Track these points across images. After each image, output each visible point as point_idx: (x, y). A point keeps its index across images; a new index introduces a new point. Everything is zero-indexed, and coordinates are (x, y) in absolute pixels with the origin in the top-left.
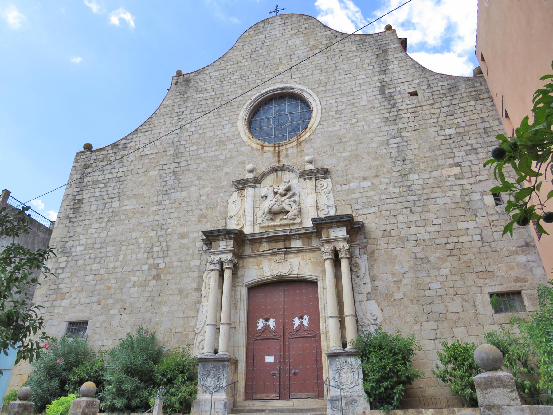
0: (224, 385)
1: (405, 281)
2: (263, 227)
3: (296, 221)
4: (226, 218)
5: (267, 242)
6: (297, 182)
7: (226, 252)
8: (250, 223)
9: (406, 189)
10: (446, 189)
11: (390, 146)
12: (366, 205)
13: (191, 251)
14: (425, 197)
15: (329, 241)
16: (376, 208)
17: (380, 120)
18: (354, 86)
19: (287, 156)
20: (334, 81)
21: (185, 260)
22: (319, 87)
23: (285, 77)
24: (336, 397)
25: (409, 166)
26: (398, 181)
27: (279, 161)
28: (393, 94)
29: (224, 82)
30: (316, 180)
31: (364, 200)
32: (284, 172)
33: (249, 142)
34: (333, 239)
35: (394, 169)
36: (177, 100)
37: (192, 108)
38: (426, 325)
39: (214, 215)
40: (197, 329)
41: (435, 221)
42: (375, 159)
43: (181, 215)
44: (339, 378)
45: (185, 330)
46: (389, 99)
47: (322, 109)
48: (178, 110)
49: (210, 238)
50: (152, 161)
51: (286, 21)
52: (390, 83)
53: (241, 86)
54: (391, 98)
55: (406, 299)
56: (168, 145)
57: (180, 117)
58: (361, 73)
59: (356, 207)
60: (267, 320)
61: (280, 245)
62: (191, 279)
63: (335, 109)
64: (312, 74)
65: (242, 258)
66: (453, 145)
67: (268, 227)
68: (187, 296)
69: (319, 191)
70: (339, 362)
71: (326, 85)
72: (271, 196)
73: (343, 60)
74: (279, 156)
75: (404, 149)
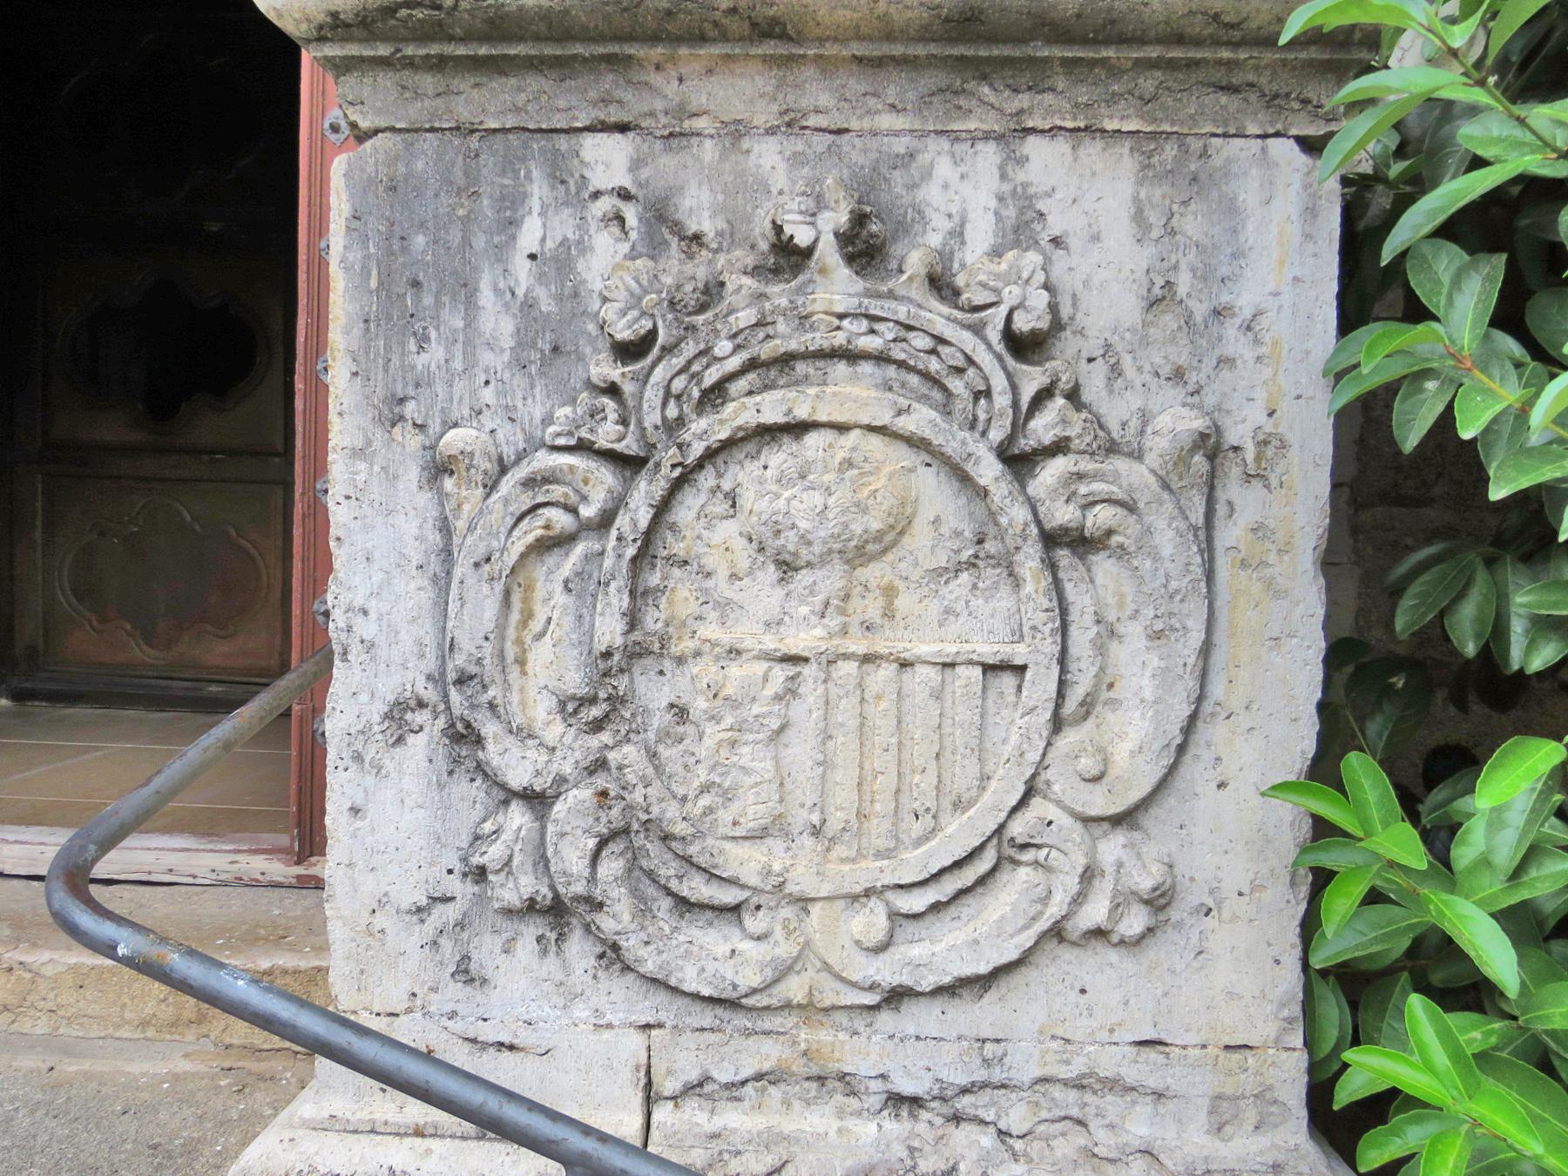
44: (600, 704)
70: (662, 224)
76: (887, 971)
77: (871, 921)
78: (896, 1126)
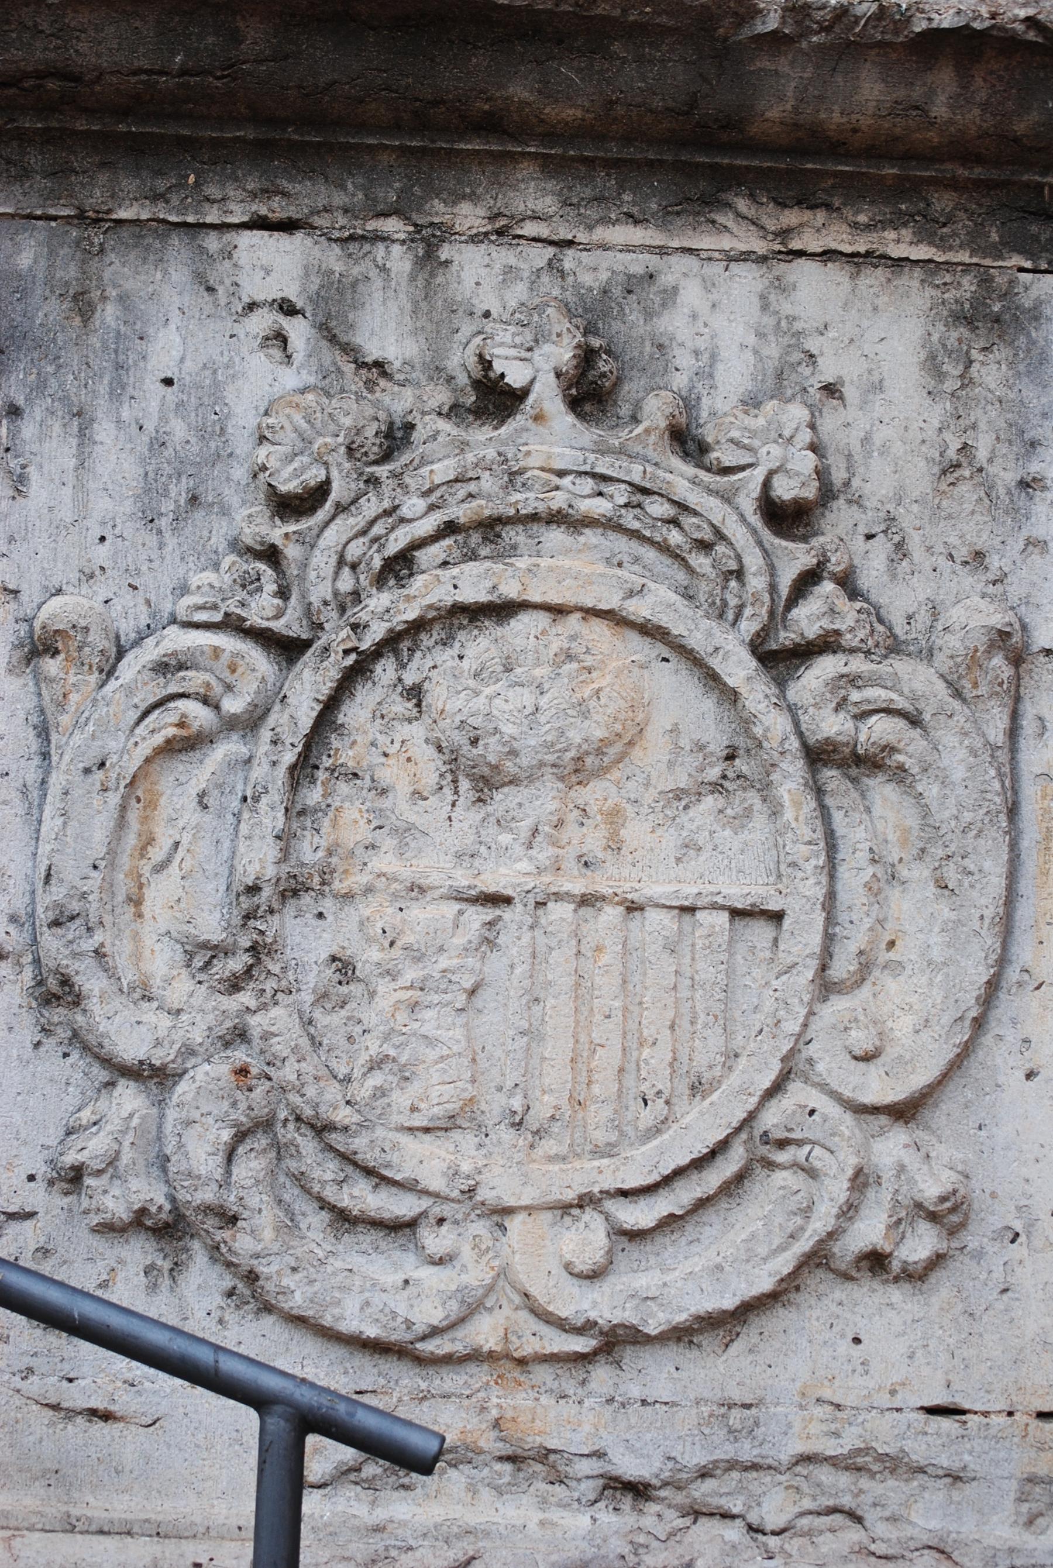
44: (242, 958)
76: (603, 1304)
77: (586, 1239)
78: (615, 1522)
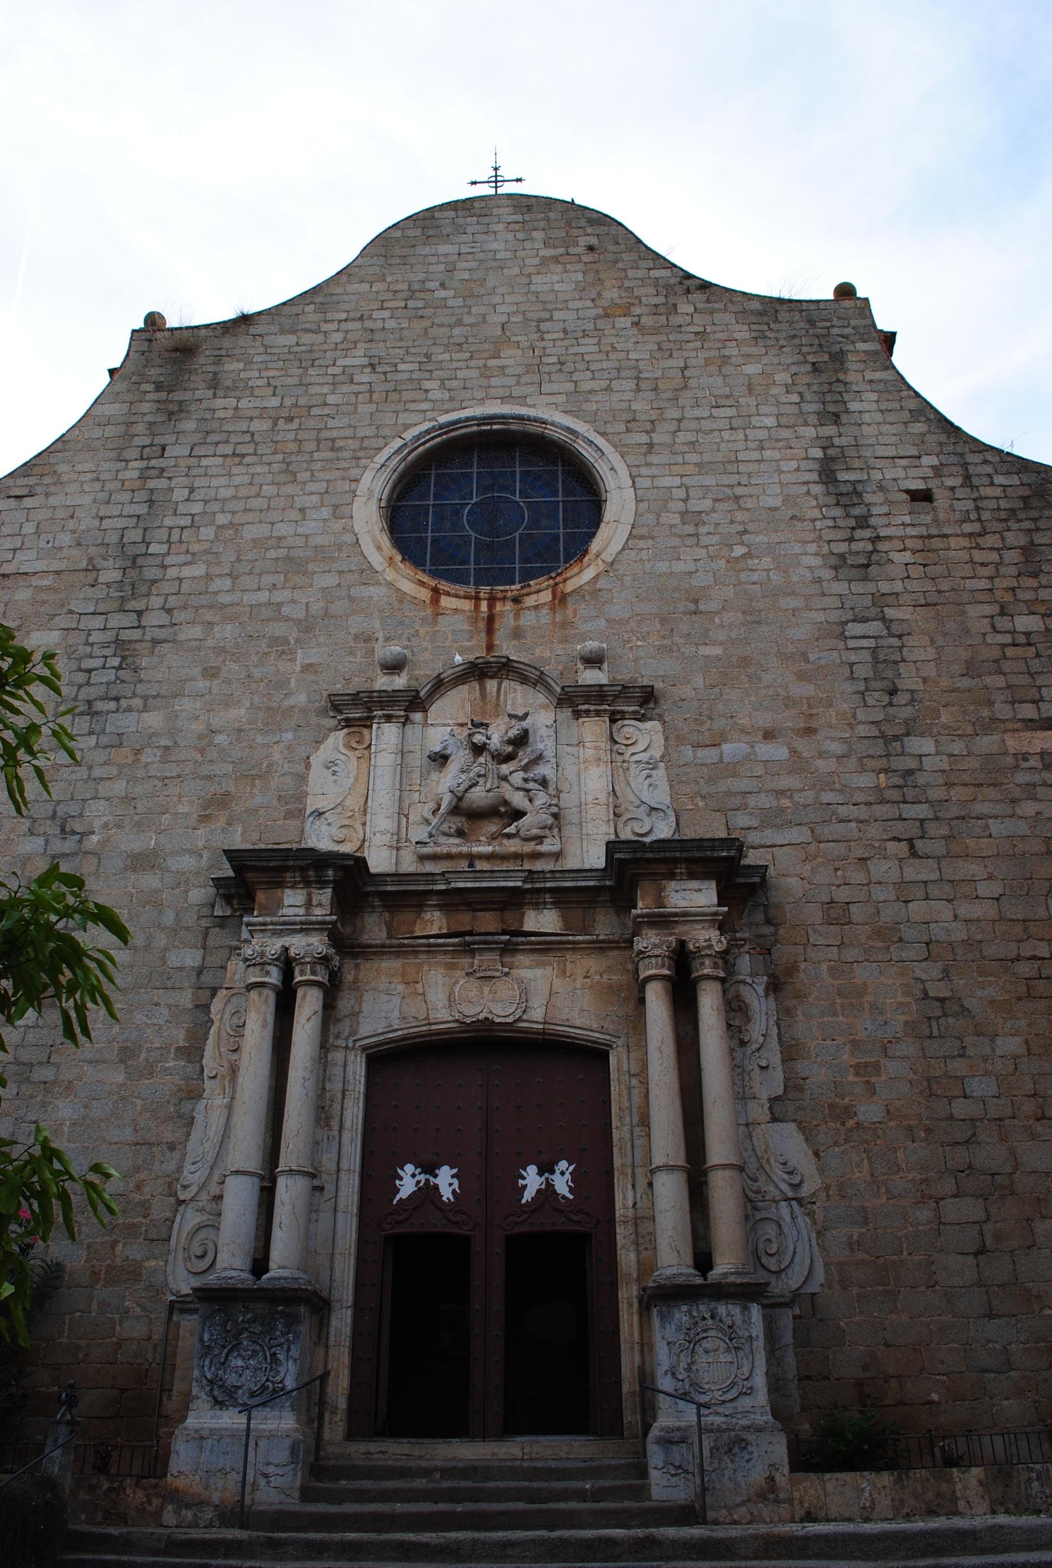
0: (290, 1383)
1: (891, 1068)
2: (435, 857)
3: (544, 848)
4: (299, 813)
5: (440, 907)
6: (550, 722)
7: (305, 928)
8: (386, 839)
9: (897, 780)
10: (1018, 793)
11: (851, 643)
12: (771, 819)
13: (169, 918)
14: (954, 811)
15: (663, 921)
16: (805, 830)
17: (817, 561)
18: (741, 445)
19: (517, 633)
20: (680, 420)
21: (147, 947)
22: (628, 431)
23: (518, 383)
24: (679, 1429)
25: (907, 712)
26: (871, 752)
27: (490, 647)
28: (859, 488)
29: (311, 371)
30: (613, 721)
31: (766, 801)
32: (505, 683)
33: (390, 575)
34: (676, 915)
35: (861, 715)
36: (146, 407)
37: (195, 438)
38: (952, 1209)
39: (258, 800)
40: (185, 1187)
41: (985, 889)
42: (801, 676)
43: (139, 790)
44: (688, 1369)
45: (138, 1187)
46: (845, 497)
47: (638, 501)
48: (147, 441)
49: (251, 877)
50: (43, 596)
51: (527, 217)
52: (850, 452)
53: (371, 392)
54: (855, 500)
55: (893, 1124)
56: (102, 550)
57: (153, 463)
58: (763, 409)
59: (741, 820)
60: (430, 1169)
61: (488, 921)
62: (165, 1012)
63: (680, 507)
64: (608, 389)
65: (355, 956)
66: (1036, 665)
67: (449, 857)
68: (150, 1070)
69: (619, 758)
71: (653, 431)
72: (460, 757)
73: (708, 362)
74: (490, 631)
75: (893, 658)
77: (720, 1393)
